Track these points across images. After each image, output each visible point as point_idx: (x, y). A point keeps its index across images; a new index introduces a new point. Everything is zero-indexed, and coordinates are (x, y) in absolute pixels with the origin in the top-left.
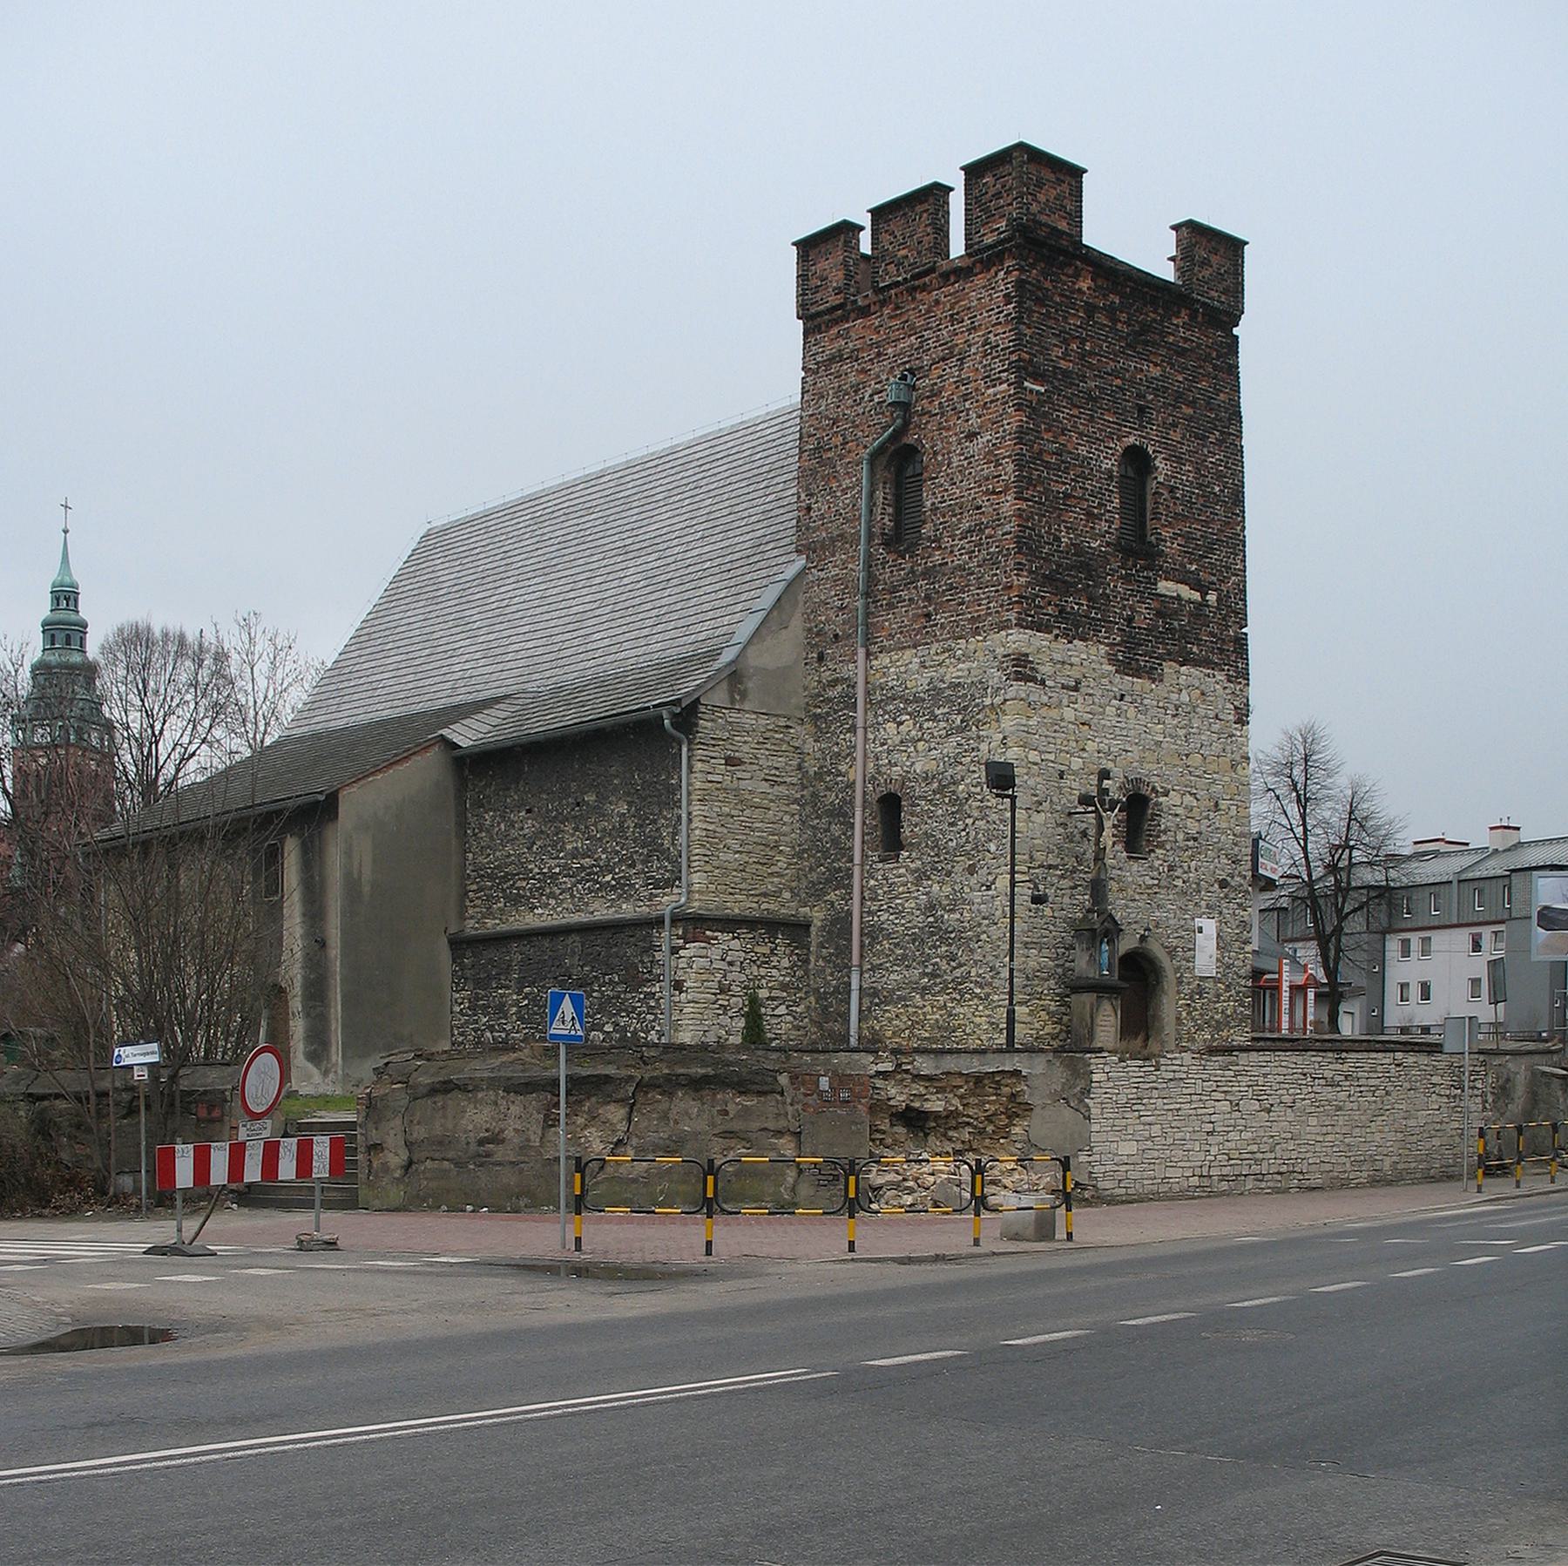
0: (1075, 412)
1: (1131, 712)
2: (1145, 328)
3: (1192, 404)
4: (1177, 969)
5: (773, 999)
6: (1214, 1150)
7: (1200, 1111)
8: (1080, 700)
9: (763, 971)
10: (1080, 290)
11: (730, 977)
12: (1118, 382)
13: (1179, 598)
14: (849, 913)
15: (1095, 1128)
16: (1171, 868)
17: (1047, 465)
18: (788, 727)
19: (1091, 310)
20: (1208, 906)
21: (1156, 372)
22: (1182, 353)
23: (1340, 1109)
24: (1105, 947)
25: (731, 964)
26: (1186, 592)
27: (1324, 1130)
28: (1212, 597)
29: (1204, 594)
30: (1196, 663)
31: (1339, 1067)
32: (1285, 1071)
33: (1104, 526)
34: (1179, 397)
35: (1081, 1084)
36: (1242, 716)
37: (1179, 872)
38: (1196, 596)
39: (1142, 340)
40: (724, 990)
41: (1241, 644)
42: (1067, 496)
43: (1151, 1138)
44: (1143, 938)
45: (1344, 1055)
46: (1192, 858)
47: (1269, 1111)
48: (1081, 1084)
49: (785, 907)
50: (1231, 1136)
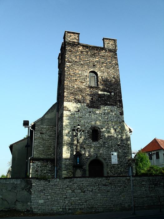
0: (78, 67)
1: (93, 115)
2: (95, 53)
3: (106, 63)
4: (107, 163)
5: (47, 173)
6: (67, 202)
7: (62, 192)
8: (79, 113)
9: (45, 168)
10: (79, 49)
11: (38, 169)
12: (88, 62)
13: (104, 94)
14: (55, 158)
15: (32, 196)
16: (104, 143)
17: (71, 75)
18: (53, 127)
19: (82, 52)
20: (115, 150)
21: (98, 59)
22: (104, 56)
23: (109, 191)
24: (78, 158)
25: (38, 167)
26: (106, 93)
27: (103, 197)
28: (113, 94)
29: (110, 93)
30: (109, 105)
31: (107, 181)
32: (89, 182)
33: (85, 84)
34: (103, 63)
35: (29, 186)
36: (122, 114)
37: (107, 143)
38: (109, 94)
39: (94, 55)
40: (37, 171)
41: (121, 101)
42: (76, 80)
43: (48, 199)
44: (97, 157)
45: (108, 178)
46: (110, 141)
48: (29, 186)
49: (52, 157)
50: (72, 198)
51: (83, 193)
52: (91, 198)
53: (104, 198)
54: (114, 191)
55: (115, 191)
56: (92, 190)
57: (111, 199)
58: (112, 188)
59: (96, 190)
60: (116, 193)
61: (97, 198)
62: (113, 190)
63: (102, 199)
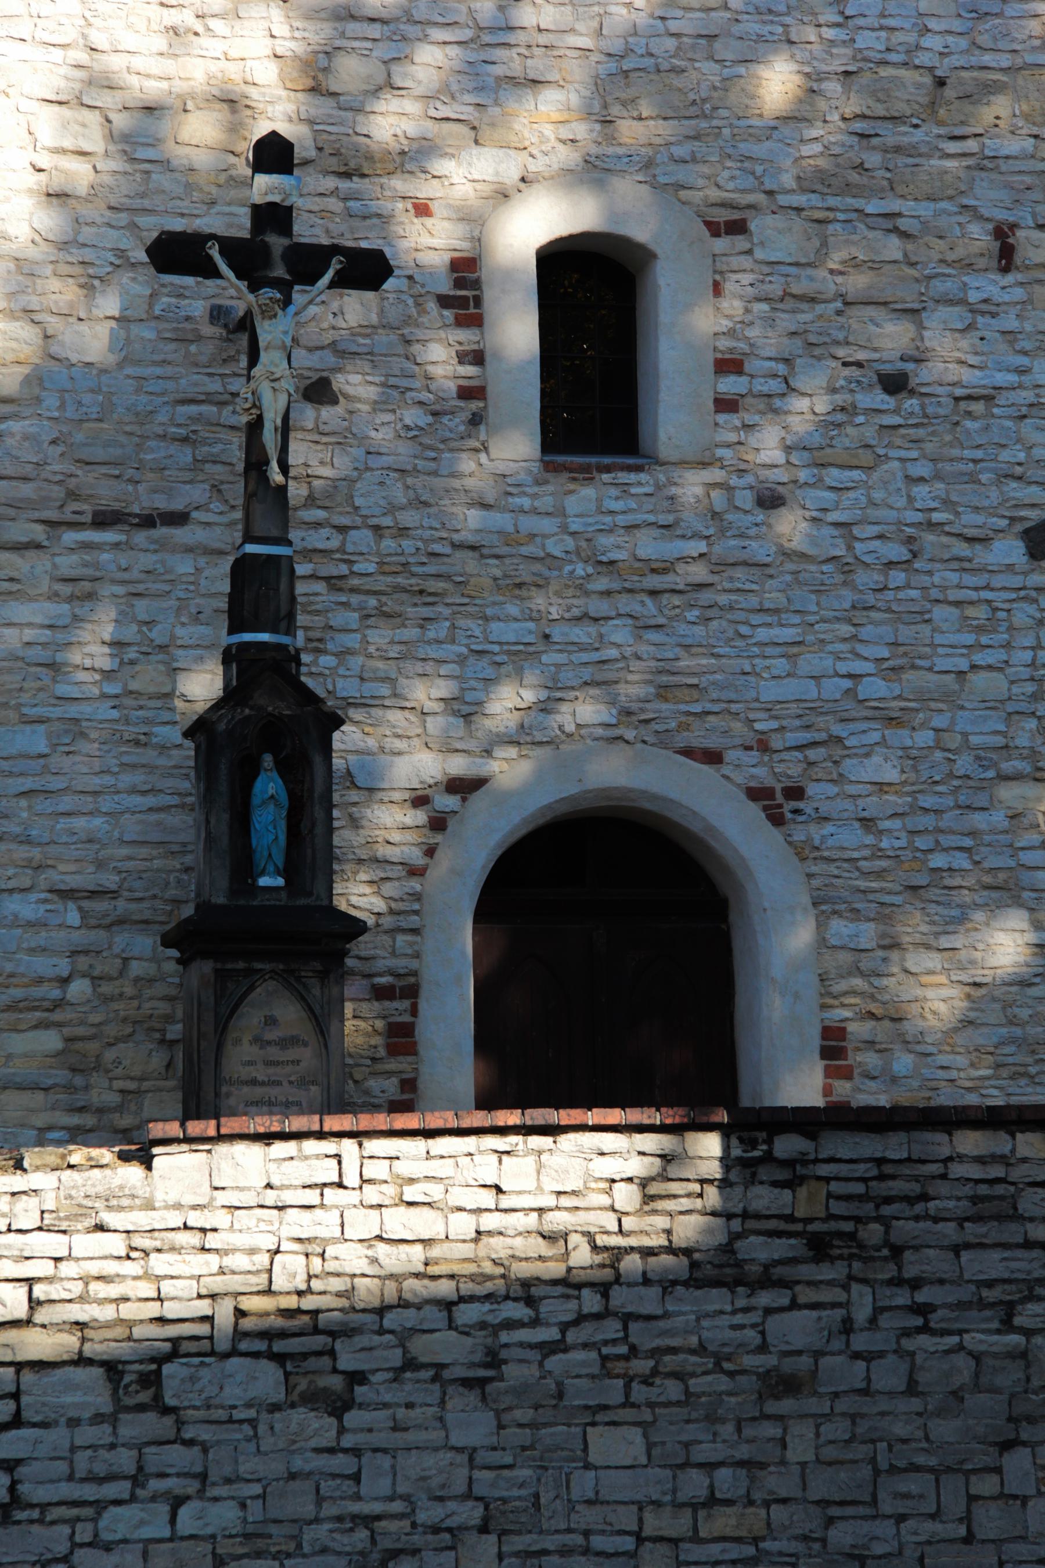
47: (339, 1406)
51: (319, 1426)
52: (470, 1513)
53: (712, 1501)
54: (889, 1375)
55: (912, 1389)
56: (494, 1360)
57: (842, 1536)
58: (847, 1327)
59: (554, 1362)
60: (944, 1429)
61: (587, 1517)
62: (868, 1357)
63: (679, 1525)
